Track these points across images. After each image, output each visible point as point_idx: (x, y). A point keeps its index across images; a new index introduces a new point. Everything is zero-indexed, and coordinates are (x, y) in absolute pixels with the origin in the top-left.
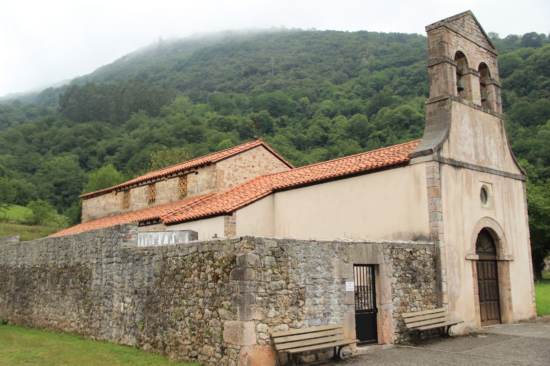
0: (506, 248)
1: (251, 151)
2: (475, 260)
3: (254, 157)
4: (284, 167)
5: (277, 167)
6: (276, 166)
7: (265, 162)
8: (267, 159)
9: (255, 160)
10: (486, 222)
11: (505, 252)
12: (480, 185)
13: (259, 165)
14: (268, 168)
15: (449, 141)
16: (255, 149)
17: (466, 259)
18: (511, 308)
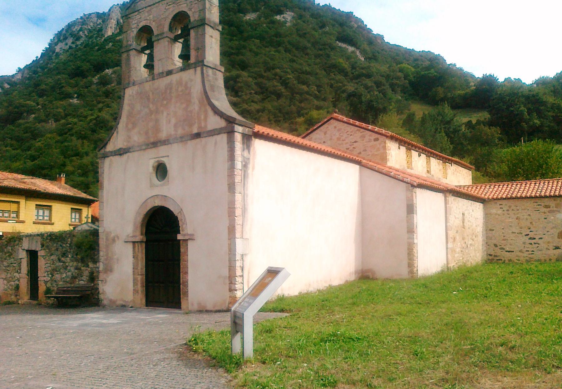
0: (184, 226)
1: (322, 128)
2: (137, 242)
3: (325, 133)
4: (361, 132)
5: (351, 135)
6: (351, 133)
7: (337, 135)
8: (339, 130)
9: (327, 135)
10: (156, 201)
11: (183, 231)
12: (151, 163)
13: (331, 139)
14: (341, 139)
15: (117, 133)
16: (325, 126)
17: (126, 242)
18: (186, 294)
